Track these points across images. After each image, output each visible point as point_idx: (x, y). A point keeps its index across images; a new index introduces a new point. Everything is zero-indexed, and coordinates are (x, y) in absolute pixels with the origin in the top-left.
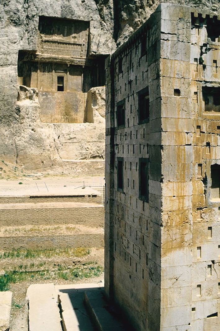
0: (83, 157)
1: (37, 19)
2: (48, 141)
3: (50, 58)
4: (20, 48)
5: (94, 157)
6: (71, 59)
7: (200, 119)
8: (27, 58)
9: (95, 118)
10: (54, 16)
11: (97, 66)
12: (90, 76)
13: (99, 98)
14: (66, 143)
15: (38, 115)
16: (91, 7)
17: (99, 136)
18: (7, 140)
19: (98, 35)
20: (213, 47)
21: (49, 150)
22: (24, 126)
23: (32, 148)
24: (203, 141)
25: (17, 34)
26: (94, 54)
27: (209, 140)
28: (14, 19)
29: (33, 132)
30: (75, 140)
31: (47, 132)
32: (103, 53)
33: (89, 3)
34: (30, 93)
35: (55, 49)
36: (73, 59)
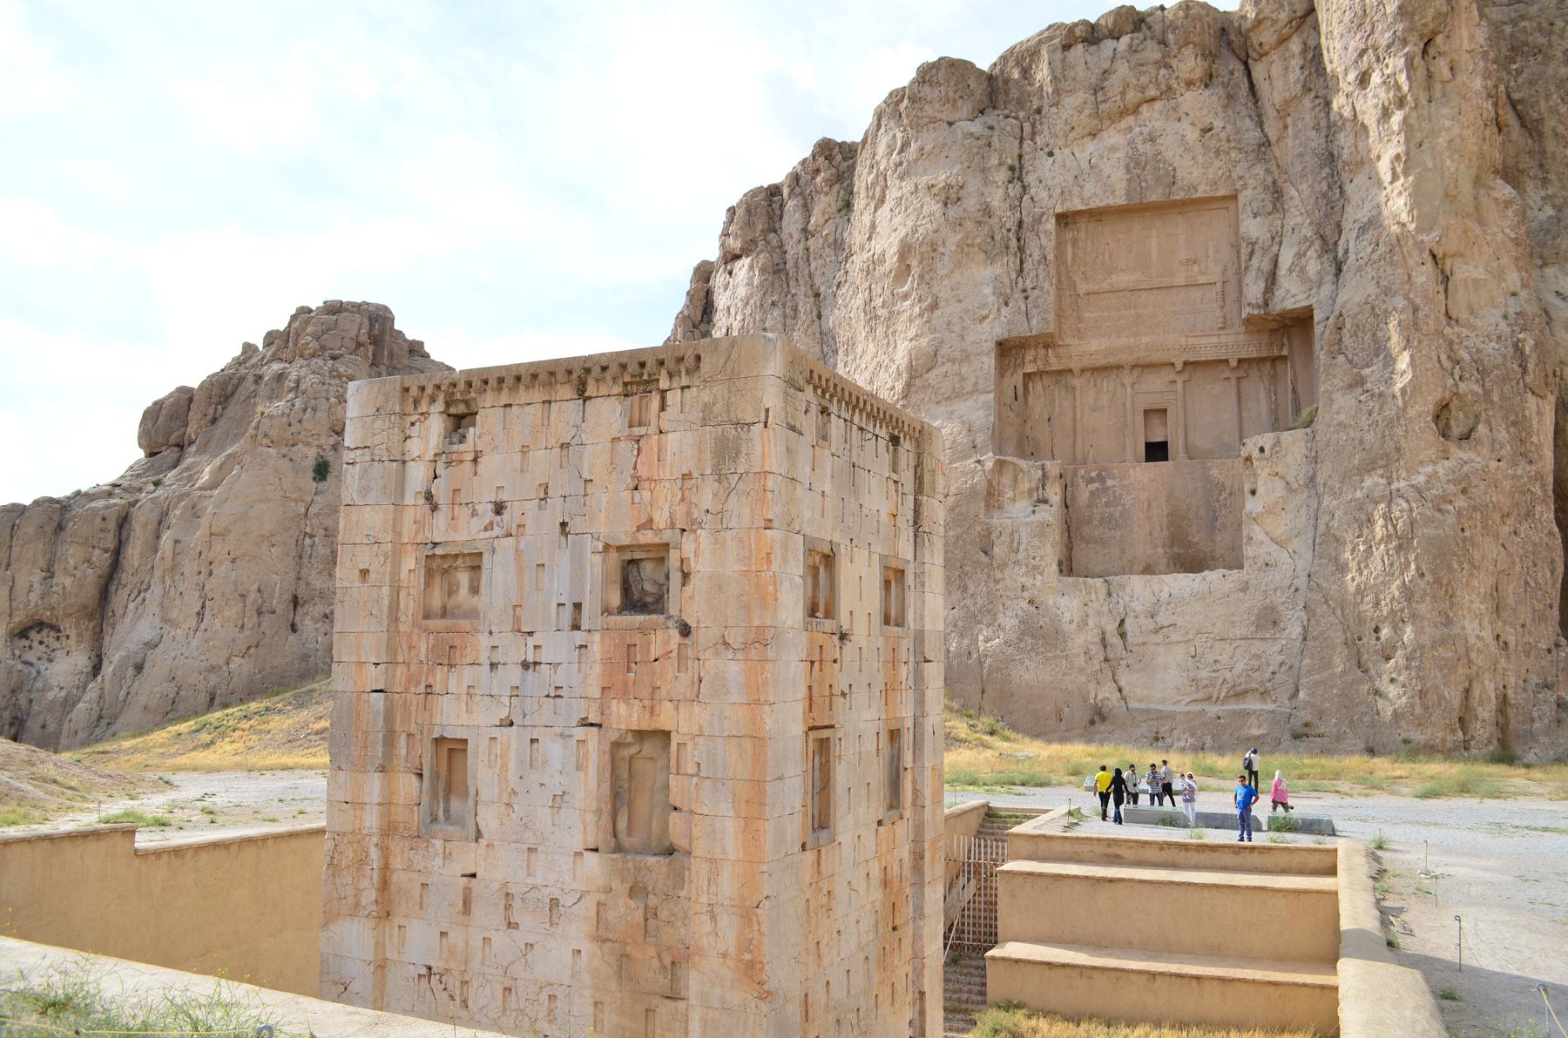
1: (1050, 225)
5: (1241, 695)
7: (416, 631)
8: (1034, 361)
9: (1249, 551)
12: (1263, 396)
14: (1144, 644)
17: (1259, 618)
20: (454, 457)
21: (1082, 670)
23: (1027, 662)
24: (418, 683)
25: (988, 290)
27: (431, 680)
28: (978, 241)
29: (1032, 609)
30: (1175, 637)
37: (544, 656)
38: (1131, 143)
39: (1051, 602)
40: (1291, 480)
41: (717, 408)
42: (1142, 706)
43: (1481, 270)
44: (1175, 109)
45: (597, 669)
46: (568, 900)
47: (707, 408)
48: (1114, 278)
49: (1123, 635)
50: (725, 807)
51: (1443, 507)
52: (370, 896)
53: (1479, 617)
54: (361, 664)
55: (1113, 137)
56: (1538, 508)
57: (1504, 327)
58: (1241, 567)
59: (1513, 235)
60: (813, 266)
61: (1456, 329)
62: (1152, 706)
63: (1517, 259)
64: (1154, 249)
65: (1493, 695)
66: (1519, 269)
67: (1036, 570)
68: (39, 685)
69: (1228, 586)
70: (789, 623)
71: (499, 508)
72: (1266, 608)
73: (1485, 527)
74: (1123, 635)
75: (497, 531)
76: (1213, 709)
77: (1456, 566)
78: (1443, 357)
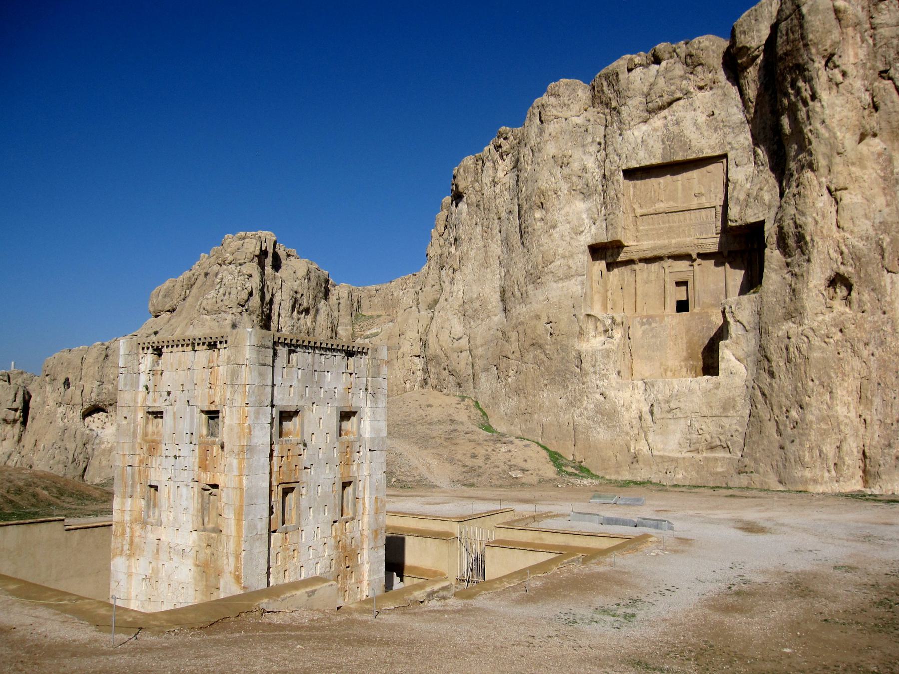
0: (692, 449)
2: (627, 416)
3: (654, 249)
4: (590, 241)
5: (712, 448)
6: (696, 241)
9: (722, 366)
10: (648, 163)
11: (755, 246)
13: (730, 319)
15: (612, 365)
16: (729, 122)
18: (562, 415)
19: (747, 179)
22: (588, 387)
25: (585, 216)
26: (734, 224)
28: (579, 187)
29: (602, 398)
31: (630, 399)
32: (752, 220)
33: (723, 113)
34: (605, 325)
35: (662, 228)
36: (700, 241)
37: (181, 454)
38: (666, 126)
39: (613, 395)
40: (745, 324)
41: (232, 358)
42: (661, 453)
43: (859, 197)
44: (691, 105)
45: (197, 459)
46: (188, 550)
47: (229, 358)
48: (657, 206)
49: (652, 413)
50: (232, 516)
51: (827, 340)
52: (126, 547)
53: (847, 405)
54: (124, 455)
55: (657, 121)
56: (888, 339)
57: (871, 232)
58: (717, 375)
59: (882, 174)
60: (498, 201)
61: (842, 233)
62: (666, 454)
63: (884, 189)
64: (680, 187)
65: (855, 450)
66: (885, 195)
67: (604, 377)
68: (97, 441)
69: (710, 386)
70: (260, 443)
71: (169, 394)
72: (730, 398)
73: (854, 352)
74: (652, 413)
75: (167, 403)
76: (699, 457)
77: (832, 375)
78: (831, 251)
